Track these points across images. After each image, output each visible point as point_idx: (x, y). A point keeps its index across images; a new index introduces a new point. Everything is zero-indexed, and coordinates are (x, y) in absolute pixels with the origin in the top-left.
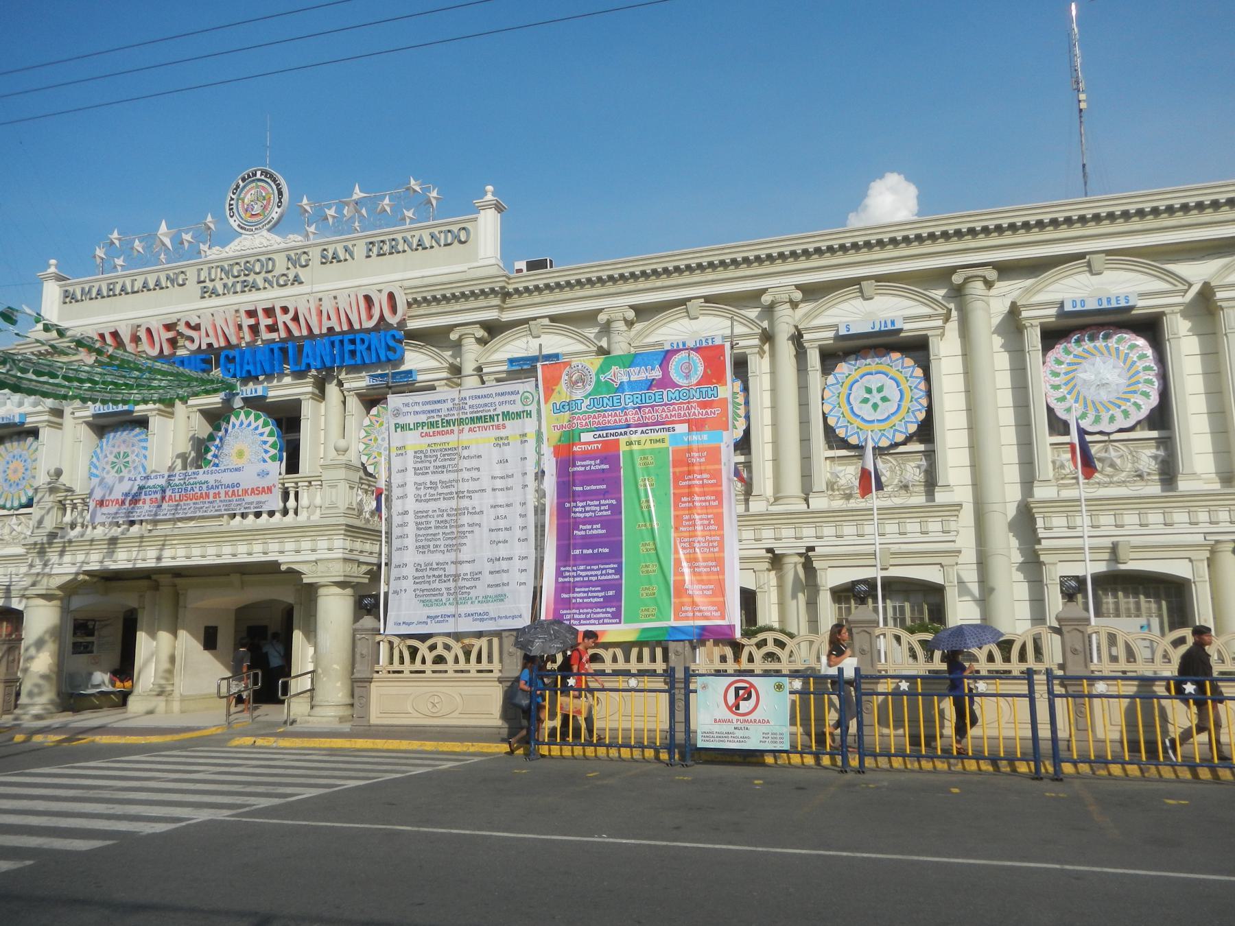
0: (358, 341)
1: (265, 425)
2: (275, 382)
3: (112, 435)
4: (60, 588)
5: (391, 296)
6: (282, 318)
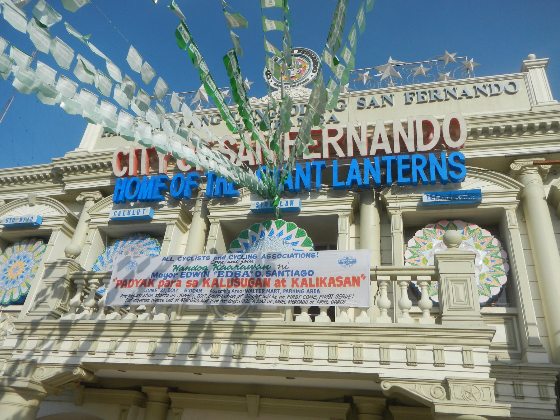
0: (414, 162)
1: (299, 235)
2: (309, 199)
3: (121, 243)
4: (45, 383)
5: (454, 124)
6: (326, 140)
